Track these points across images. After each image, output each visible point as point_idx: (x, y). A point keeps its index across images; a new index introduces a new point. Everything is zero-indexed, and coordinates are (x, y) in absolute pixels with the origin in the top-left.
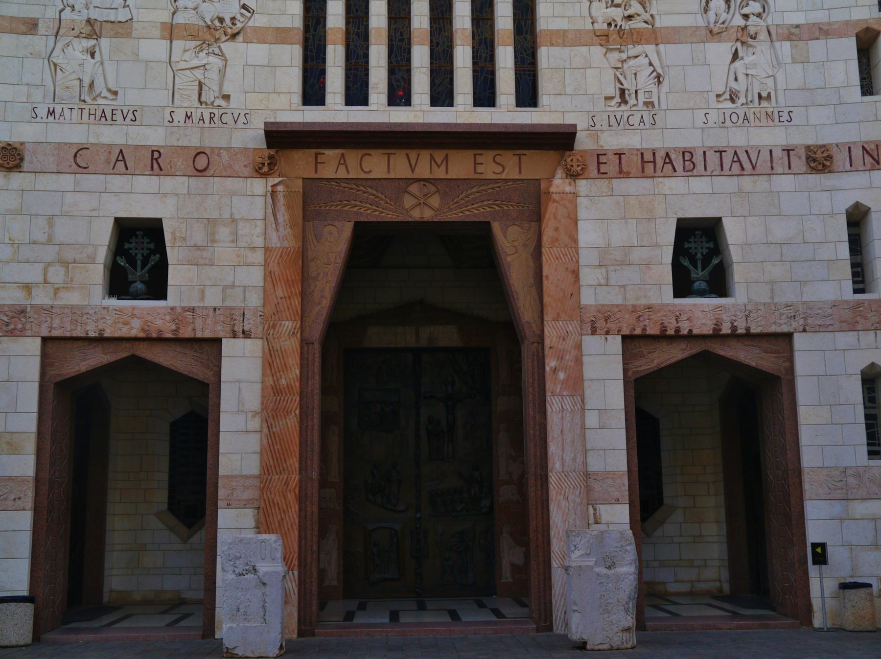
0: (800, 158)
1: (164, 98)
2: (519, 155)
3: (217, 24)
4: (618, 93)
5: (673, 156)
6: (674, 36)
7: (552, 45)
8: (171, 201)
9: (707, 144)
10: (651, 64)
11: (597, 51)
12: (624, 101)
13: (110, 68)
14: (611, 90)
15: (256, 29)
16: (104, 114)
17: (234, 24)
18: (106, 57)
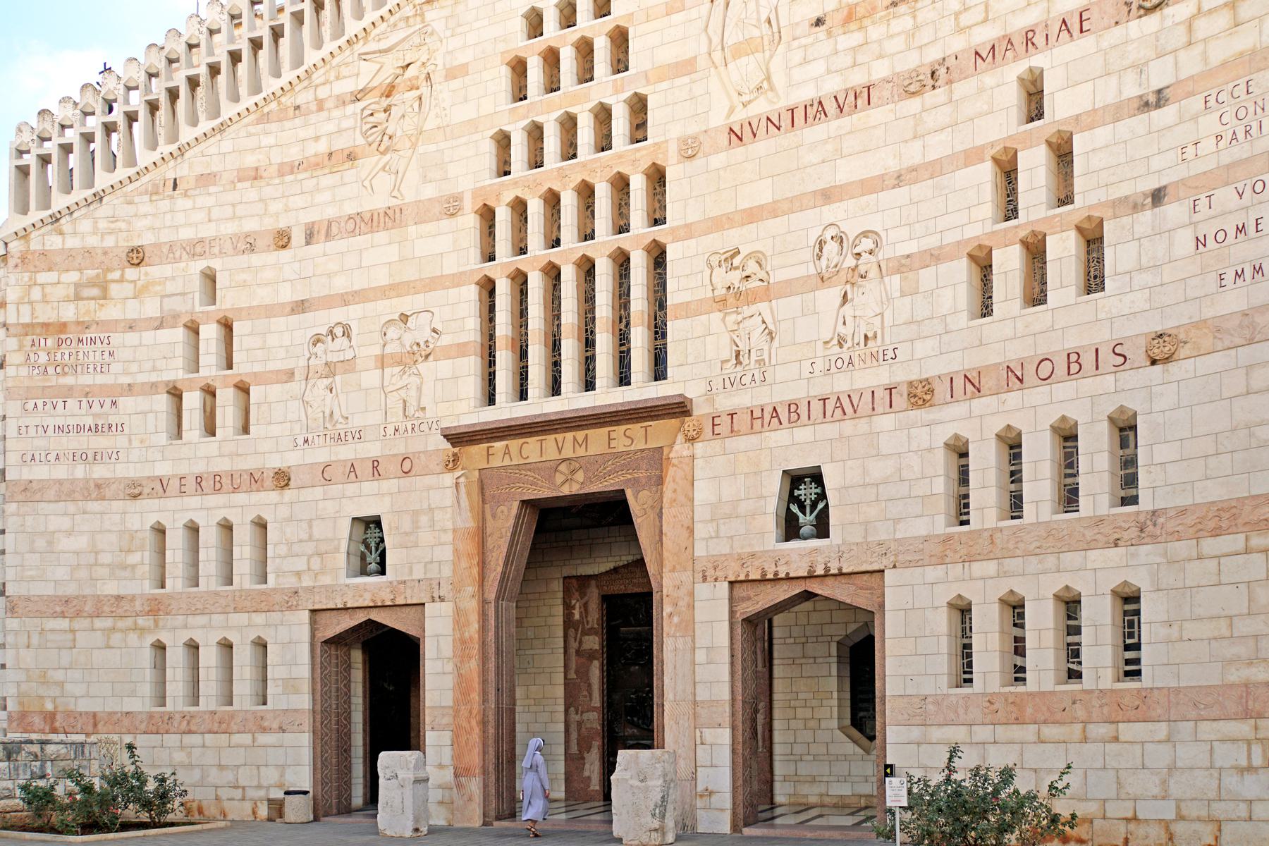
0: (901, 395)
1: (378, 418)
2: (646, 427)
3: (415, 348)
4: (734, 355)
5: (779, 410)
6: (789, 288)
7: (676, 318)
8: (387, 500)
9: (812, 393)
10: (764, 322)
11: (717, 316)
12: (739, 362)
13: (342, 397)
14: (727, 353)
15: (444, 348)
16: (340, 438)
17: (427, 346)
18: (339, 391)
